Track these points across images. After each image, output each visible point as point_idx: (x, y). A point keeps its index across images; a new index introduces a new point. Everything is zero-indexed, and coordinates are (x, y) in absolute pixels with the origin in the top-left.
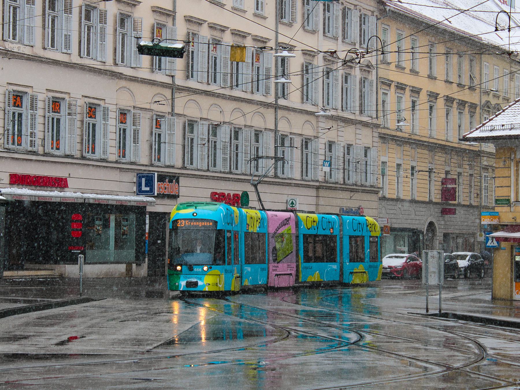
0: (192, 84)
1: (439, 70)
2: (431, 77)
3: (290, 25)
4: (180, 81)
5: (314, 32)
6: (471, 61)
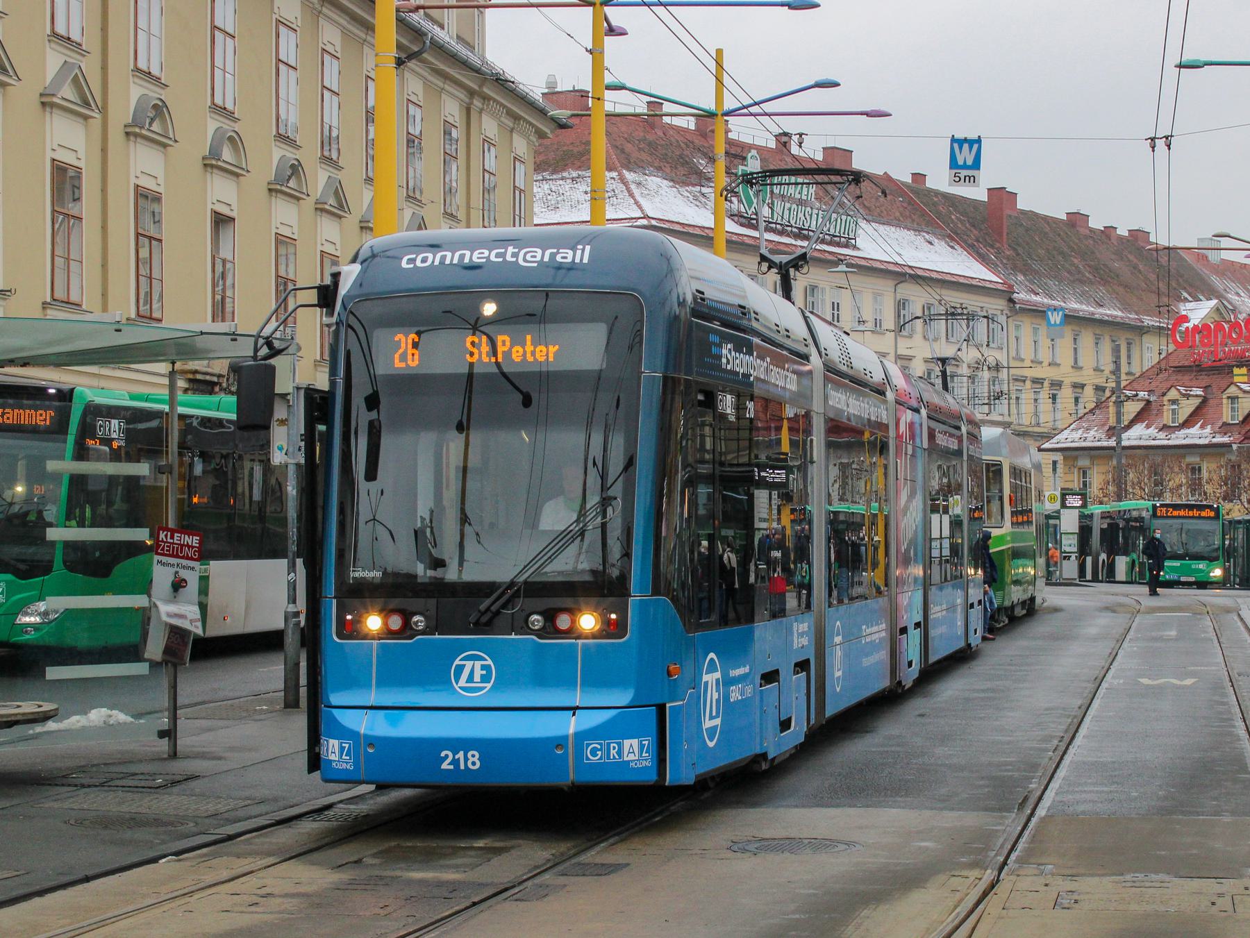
1: (1087, 360)
2: (1076, 367)
3: (910, 336)
6: (1129, 344)
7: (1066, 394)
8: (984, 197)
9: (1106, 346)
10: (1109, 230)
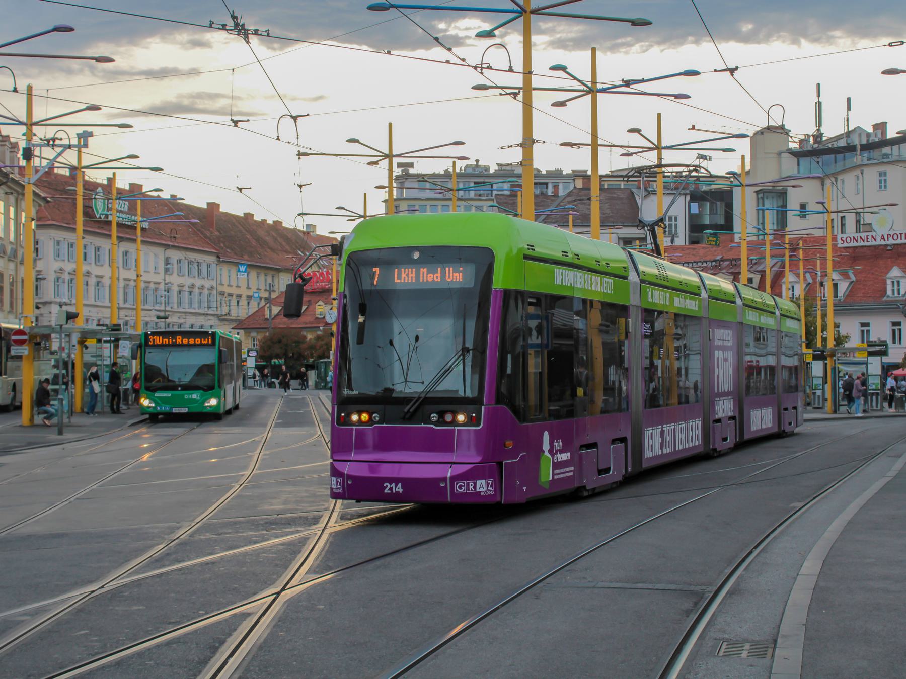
0: (127, 306)
1: (254, 284)
2: (248, 288)
4: (122, 305)
5: (183, 276)
7: (243, 302)
8: (205, 206)
9: (262, 277)
10: (264, 221)
